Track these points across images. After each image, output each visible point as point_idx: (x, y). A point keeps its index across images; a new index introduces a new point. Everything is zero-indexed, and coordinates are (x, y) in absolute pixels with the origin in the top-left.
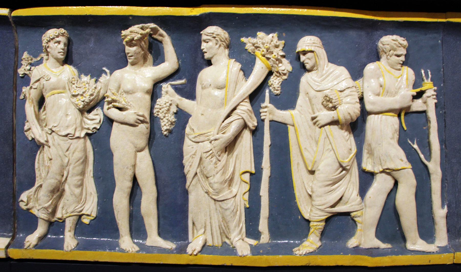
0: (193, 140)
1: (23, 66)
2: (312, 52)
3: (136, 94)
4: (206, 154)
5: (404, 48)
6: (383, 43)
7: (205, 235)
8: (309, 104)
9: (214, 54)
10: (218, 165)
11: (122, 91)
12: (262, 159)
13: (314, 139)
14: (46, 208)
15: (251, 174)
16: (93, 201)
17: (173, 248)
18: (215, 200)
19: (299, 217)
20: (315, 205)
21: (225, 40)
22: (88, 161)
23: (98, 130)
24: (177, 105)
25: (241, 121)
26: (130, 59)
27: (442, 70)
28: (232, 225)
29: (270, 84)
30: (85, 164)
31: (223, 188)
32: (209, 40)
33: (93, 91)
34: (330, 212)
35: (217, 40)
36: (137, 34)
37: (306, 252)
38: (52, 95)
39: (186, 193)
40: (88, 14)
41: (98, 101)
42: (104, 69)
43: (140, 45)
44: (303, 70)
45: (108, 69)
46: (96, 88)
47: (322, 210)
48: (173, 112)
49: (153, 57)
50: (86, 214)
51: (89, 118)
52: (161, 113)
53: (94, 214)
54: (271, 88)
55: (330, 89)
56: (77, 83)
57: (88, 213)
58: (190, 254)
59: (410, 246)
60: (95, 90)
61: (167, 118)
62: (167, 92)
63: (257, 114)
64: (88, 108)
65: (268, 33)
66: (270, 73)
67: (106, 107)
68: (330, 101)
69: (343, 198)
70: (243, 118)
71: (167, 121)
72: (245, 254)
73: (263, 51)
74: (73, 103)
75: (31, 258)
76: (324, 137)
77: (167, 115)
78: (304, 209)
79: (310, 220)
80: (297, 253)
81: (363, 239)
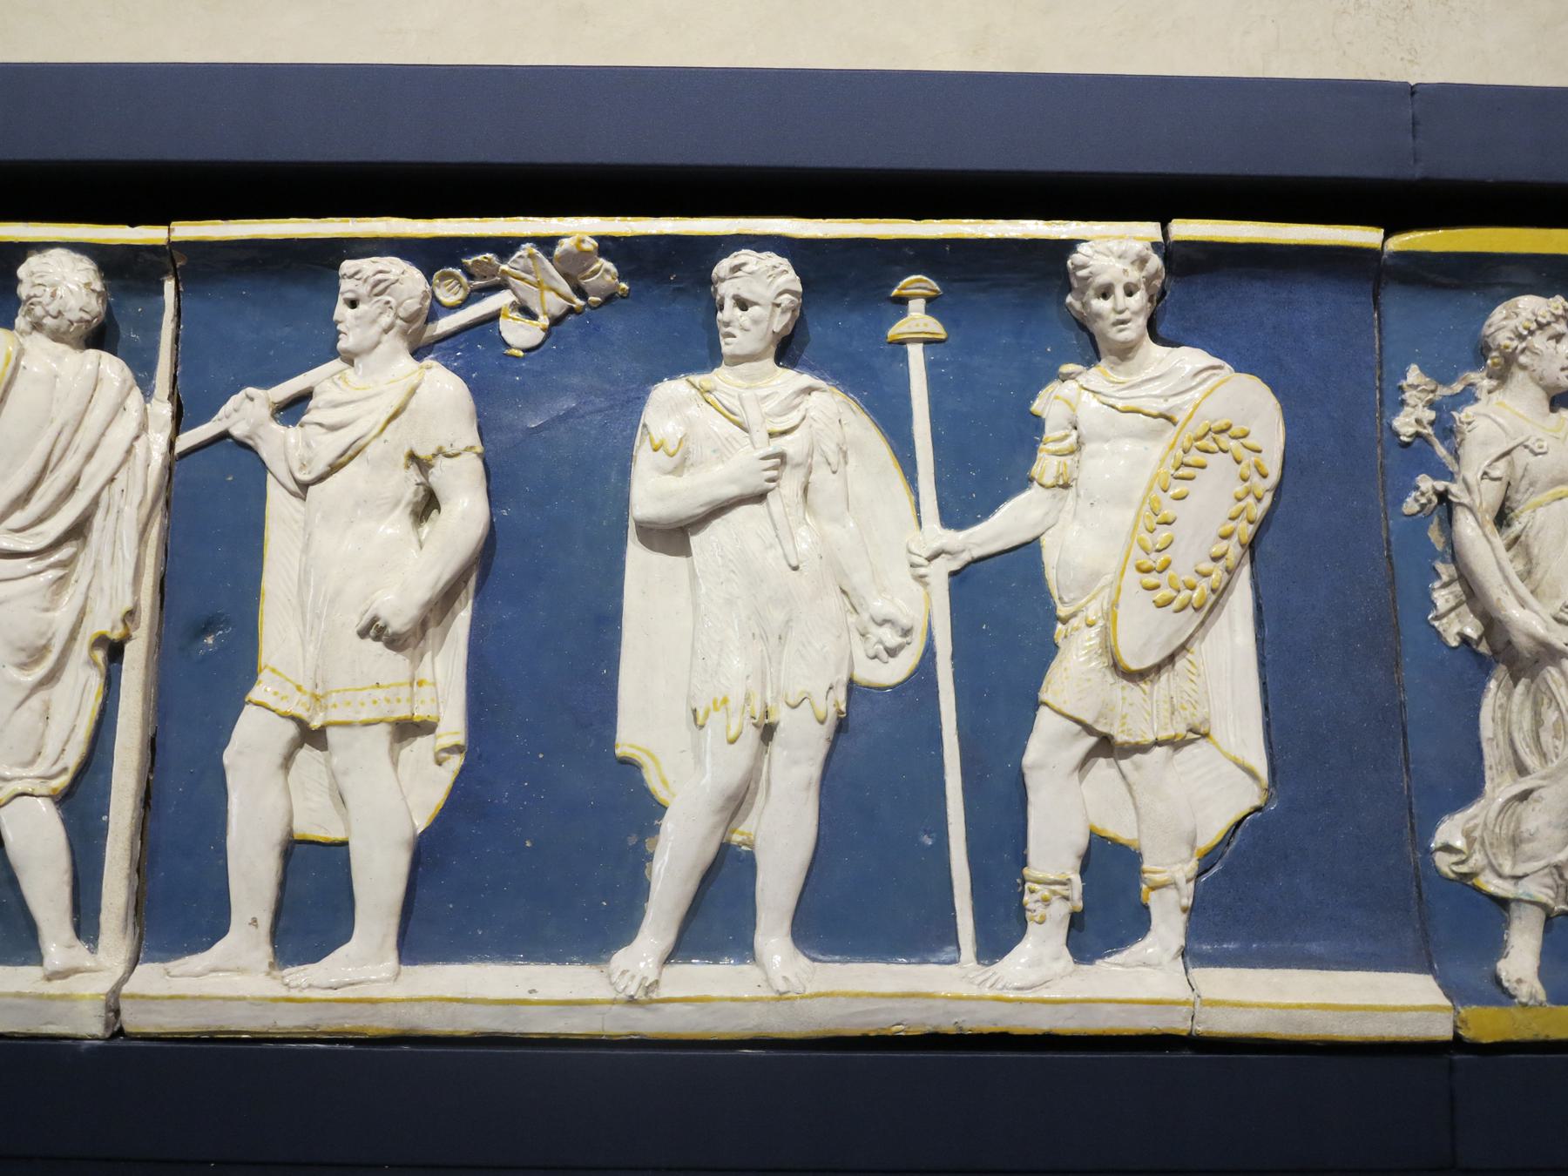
1: (1407, 409)
38: (1554, 500)
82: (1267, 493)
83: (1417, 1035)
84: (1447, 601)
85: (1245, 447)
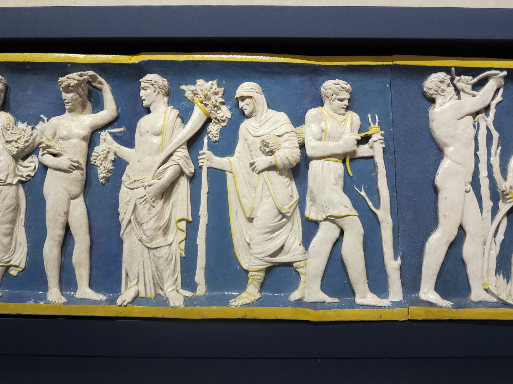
0: (128, 186)
2: (250, 97)
3: (71, 140)
4: (140, 200)
5: (347, 92)
6: (325, 88)
7: (138, 286)
8: (248, 150)
9: (152, 101)
10: (152, 211)
11: (58, 137)
12: (200, 207)
13: (253, 186)
15: (188, 222)
16: (23, 251)
17: (103, 300)
18: (148, 248)
19: (238, 268)
20: (253, 254)
21: (163, 87)
22: (20, 209)
23: (33, 177)
24: (114, 152)
25: (177, 167)
26: (67, 106)
27: (391, 114)
28: (166, 275)
29: (208, 130)
30: (17, 212)
31: (157, 235)
32: (147, 87)
33: (29, 137)
34: (270, 261)
35: (155, 87)
36: (73, 80)
37: (242, 304)
39: (121, 242)
40: (26, 61)
41: (34, 148)
42: (42, 116)
43: (77, 92)
44: (242, 116)
45: (46, 117)
46: (31, 135)
47: (261, 259)
48: (111, 160)
49: (93, 106)
50: (14, 264)
51: (24, 165)
52: (98, 161)
53: (23, 266)
54: (209, 135)
55: (269, 134)
56: (12, 129)
57: (17, 264)
58: (119, 305)
59: (359, 300)
60: (31, 137)
61: (104, 165)
62: (105, 140)
63: (195, 161)
64: (23, 155)
66: (209, 120)
67: (41, 153)
68: (266, 145)
69: (285, 247)
70: (178, 164)
71: (103, 168)
72: (177, 305)
73: (201, 97)
74: (6, 149)
76: (262, 183)
77: (104, 162)
78: (242, 259)
79: (248, 270)
80: (232, 304)
81: (307, 292)
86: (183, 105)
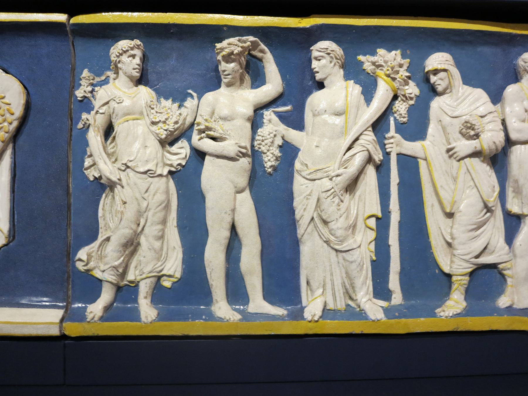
0: (308, 177)
1: (82, 87)
2: (445, 70)
3: (235, 121)
4: (327, 194)
6: (525, 60)
7: (324, 296)
8: (442, 133)
9: (328, 74)
10: (341, 207)
11: (218, 117)
12: (389, 200)
13: (450, 175)
14: (115, 268)
15: (378, 219)
16: (177, 257)
17: (284, 314)
18: (337, 251)
19: (437, 271)
20: (458, 255)
21: (341, 57)
22: (171, 206)
23: (183, 166)
24: (282, 136)
25: (366, 153)
26: (225, 78)
28: (358, 282)
29: (395, 110)
30: (167, 211)
31: (348, 236)
32: (322, 57)
33: (178, 118)
34: (476, 263)
35: (331, 57)
36: (237, 47)
37: (453, 314)
38: (125, 122)
40: (171, 22)
41: (184, 131)
42: (190, 91)
43: (239, 61)
44: (432, 94)
45: (195, 92)
46: (180, 114)
47: (467, 261)
48: (278, 145)
49: (251, 79)
50: (168, 274)
51: (172, 152)
52: (264, 146)
53: (178, 275)
54: (396, 115)
55: (469, 114)
56: (156, 108)
57: (170, 273)
58: (310, 320)
60: (180, 117)
61: (272, 151)
62: (270, 121)
63: (383, 146)
64: (170, 139)
65: (390, 51)
66: (395, 97)
67: (195, 137)
69: (489, 246)
70: (368, 150)
71: (271, 155)
72: (379, 318)
73: (388, 70)
74: (152, 132)
75: (96, 335)
76: (464, 172)
77: (271, 148)
78: (442, 261)
79: (451, 273)
80: (442, 314)
81: (516, 298)
82: (15, 121)
83: (44, 334)
84: (89, 163)
85: (2, 103)
86: (362, 78)
